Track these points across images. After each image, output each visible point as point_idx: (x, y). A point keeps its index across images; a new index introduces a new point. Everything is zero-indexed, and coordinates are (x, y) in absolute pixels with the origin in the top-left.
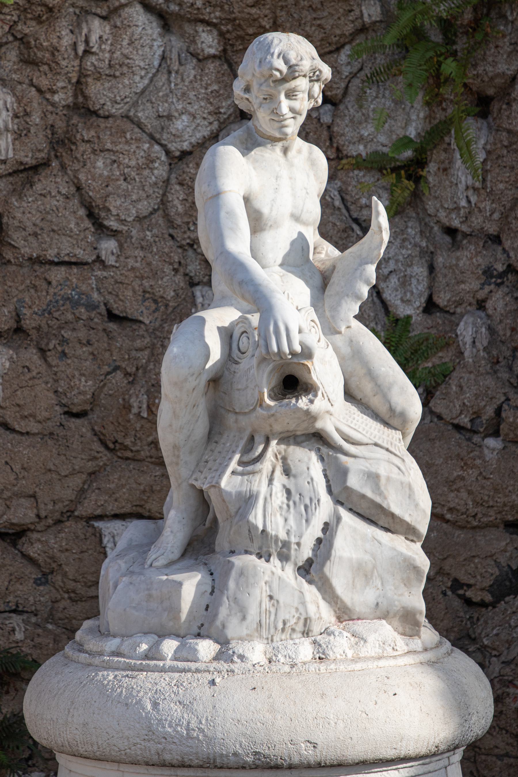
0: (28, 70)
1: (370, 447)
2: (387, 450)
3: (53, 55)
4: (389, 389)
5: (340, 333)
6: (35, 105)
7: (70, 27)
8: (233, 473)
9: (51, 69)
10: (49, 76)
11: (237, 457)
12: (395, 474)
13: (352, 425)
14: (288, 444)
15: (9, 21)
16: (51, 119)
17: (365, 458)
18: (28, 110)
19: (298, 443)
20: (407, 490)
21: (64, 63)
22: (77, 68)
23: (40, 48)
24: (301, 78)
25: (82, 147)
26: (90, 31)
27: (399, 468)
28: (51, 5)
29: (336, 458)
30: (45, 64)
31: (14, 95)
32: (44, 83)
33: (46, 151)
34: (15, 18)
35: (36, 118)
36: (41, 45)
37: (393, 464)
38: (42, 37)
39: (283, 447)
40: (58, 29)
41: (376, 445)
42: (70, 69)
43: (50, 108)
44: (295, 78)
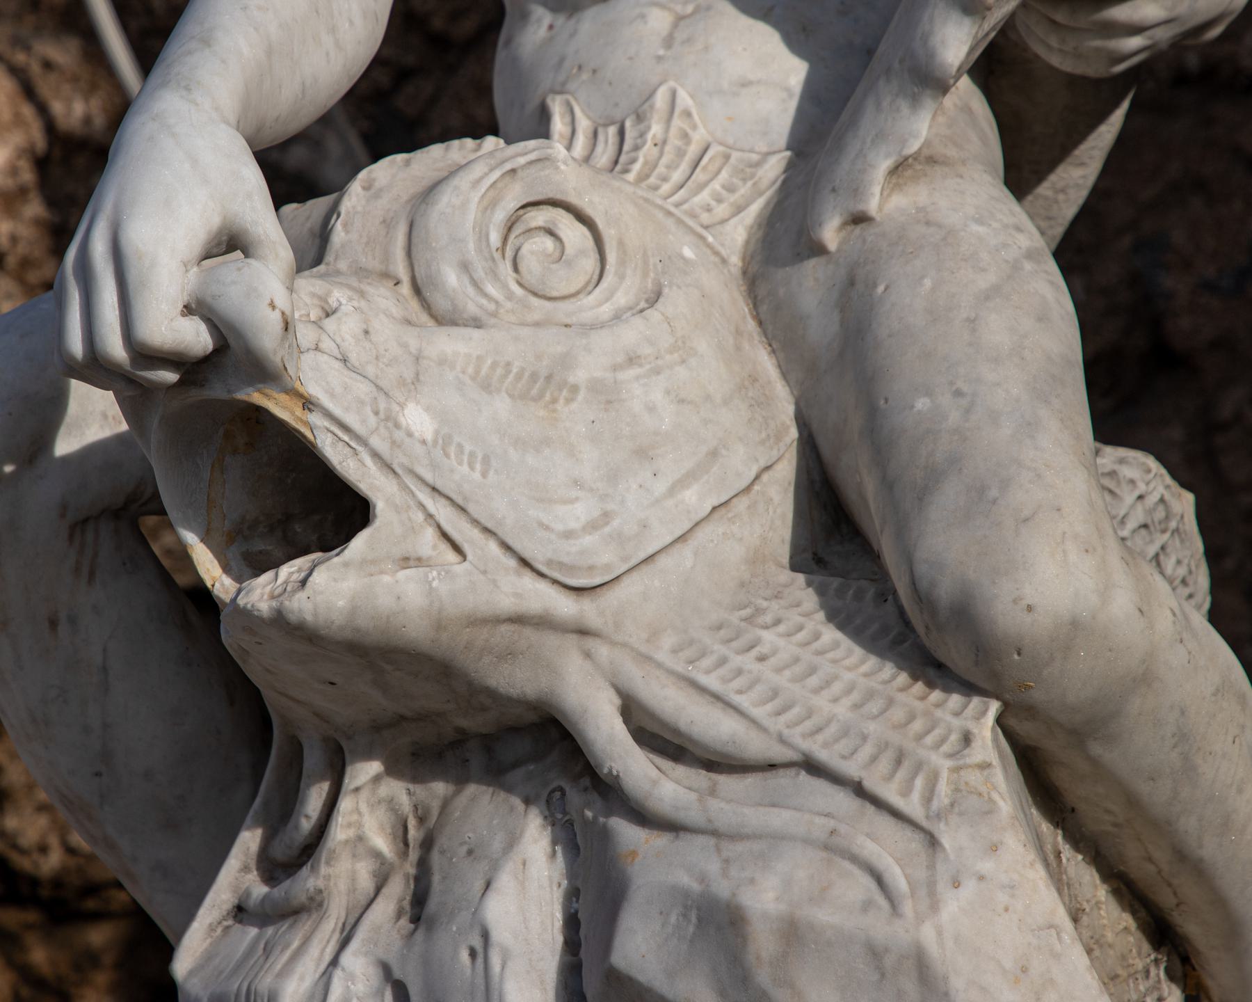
1: (783, 780)
2: (859, 791)
4: (923, 494)
5: (819, 250)
8: (240, 912)
11: (249, 840)
12: (843, 905)
13: (711, 681)
14: (461, 781)
17: (715, 833)
19: (496, 773)
20: (910, 986)
27: (879, 879)
29: (605, 836)
37: (855, 859)
39: (440, 788)
41: (813, 767)
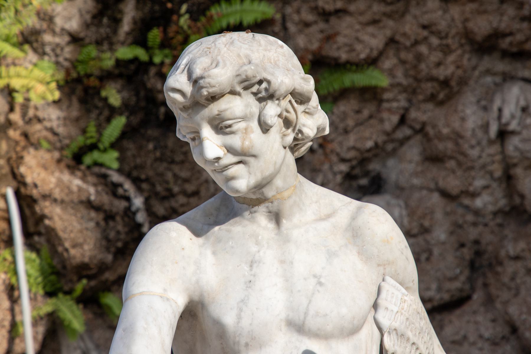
0: (434, 171)
3: (457, 144)
6: (439, 215)
7: (483, 103)
9: (460, 164)
10: (459, 173)
15: (398, 108)
16: (473, 233)
18: (427, 223)
21: (474, 153)
22: (498, 158)
23: (440, 137)
24: (228, 97)
25: (510, 267)
26: (504, 101)
28: (442, 78)
30: (451, 158)
31: (407, 206)
32: (453, 184)
33: (463, 278)
34: (403, 103)
35: (440, 234)
36: (440, 132)
38: (441, 124)
40: (460, 107)
42: (485, 159)
43: (470, 218)
44: (213, 98)
